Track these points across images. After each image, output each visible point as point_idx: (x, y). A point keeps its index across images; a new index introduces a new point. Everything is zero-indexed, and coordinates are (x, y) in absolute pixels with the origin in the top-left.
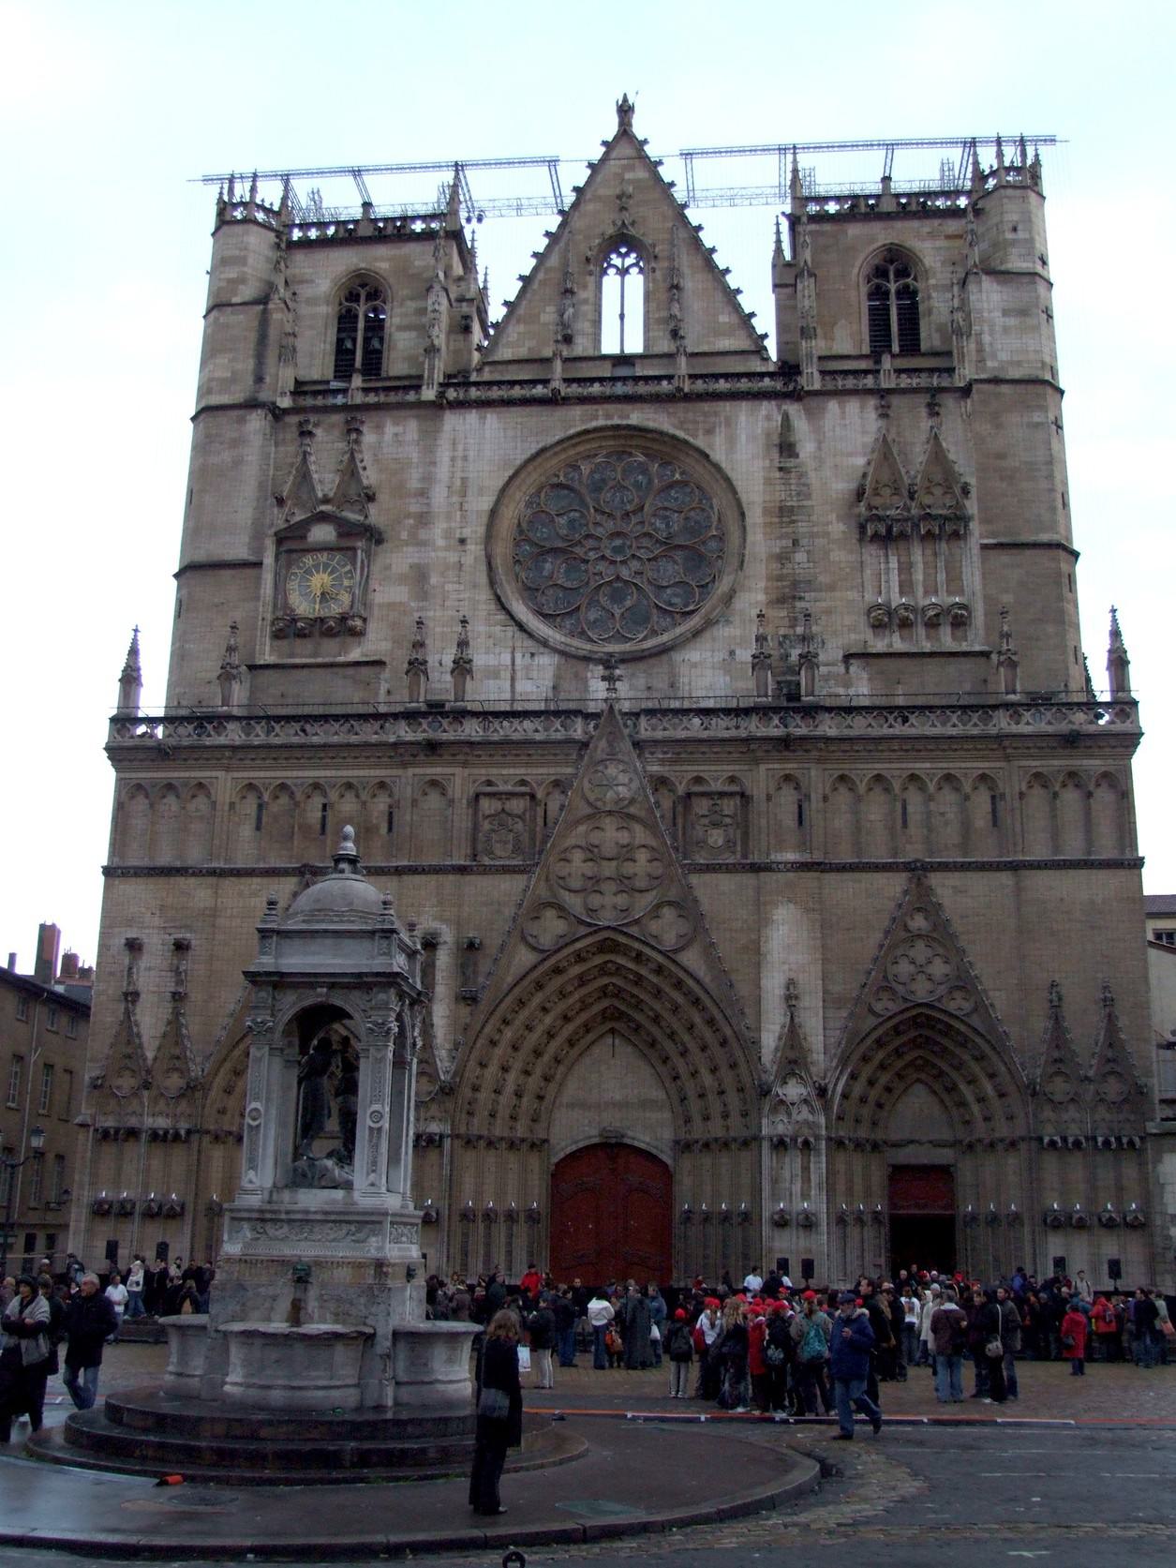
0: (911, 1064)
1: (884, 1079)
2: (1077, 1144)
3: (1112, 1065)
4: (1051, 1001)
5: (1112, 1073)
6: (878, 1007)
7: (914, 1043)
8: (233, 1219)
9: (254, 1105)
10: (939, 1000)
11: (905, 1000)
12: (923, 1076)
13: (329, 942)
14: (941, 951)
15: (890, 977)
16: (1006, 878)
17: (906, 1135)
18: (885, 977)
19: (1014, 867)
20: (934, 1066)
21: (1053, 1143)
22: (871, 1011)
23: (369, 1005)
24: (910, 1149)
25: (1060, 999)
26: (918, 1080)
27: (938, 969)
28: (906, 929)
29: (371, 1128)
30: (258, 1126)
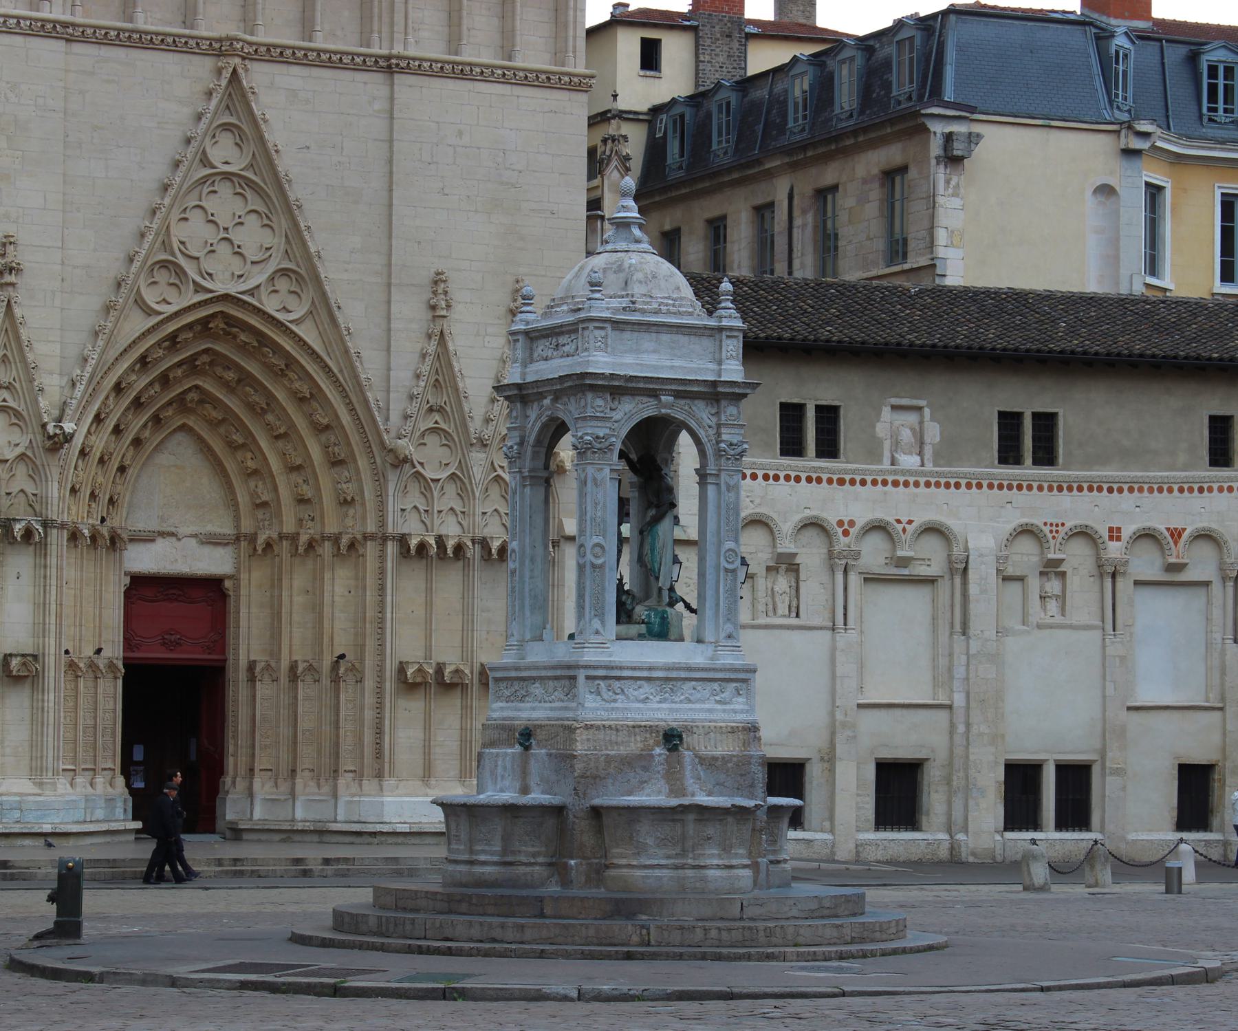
0: (180, 399)
1: (136, 424)
2: (459, 548)
3: (437, 417)
4: (433, 308)
5: (434, 430)
6: (150, 297)
7: (191, 365)
8: (588, 678)
9: (596, 540)
10: (251, 292)
11: (199, 288)
12: (191, 421)
13: (665, 337)
14: (261, 208)
15: (176, 245)
16: (374, 83)
17: (154, 526)
18: (166, 246)
19: (390, 67)
20: (216, 403)
21: (422, 547)
22: (140, 303)
23: (714, 419)
24: (161, 545)
25: (448, 306)
26: (183, 428)
27: (252, 236)
28: (205, 161)
29: (727, 570)
30: (601, 566)
